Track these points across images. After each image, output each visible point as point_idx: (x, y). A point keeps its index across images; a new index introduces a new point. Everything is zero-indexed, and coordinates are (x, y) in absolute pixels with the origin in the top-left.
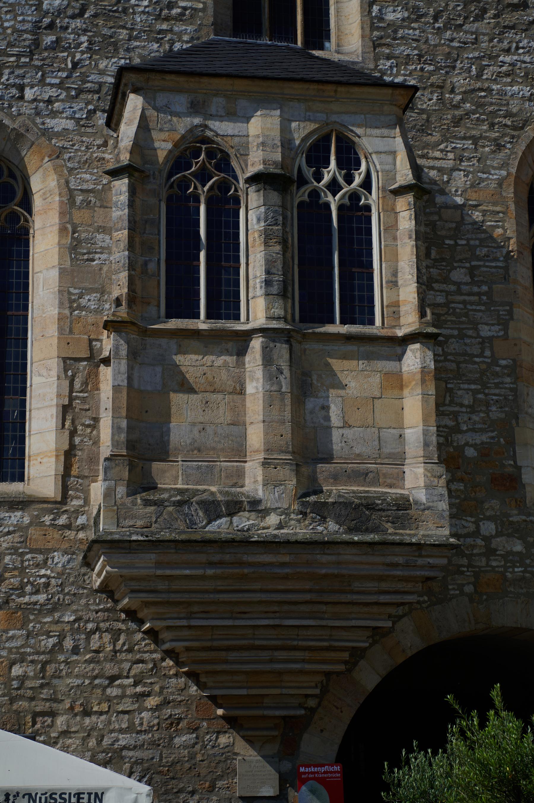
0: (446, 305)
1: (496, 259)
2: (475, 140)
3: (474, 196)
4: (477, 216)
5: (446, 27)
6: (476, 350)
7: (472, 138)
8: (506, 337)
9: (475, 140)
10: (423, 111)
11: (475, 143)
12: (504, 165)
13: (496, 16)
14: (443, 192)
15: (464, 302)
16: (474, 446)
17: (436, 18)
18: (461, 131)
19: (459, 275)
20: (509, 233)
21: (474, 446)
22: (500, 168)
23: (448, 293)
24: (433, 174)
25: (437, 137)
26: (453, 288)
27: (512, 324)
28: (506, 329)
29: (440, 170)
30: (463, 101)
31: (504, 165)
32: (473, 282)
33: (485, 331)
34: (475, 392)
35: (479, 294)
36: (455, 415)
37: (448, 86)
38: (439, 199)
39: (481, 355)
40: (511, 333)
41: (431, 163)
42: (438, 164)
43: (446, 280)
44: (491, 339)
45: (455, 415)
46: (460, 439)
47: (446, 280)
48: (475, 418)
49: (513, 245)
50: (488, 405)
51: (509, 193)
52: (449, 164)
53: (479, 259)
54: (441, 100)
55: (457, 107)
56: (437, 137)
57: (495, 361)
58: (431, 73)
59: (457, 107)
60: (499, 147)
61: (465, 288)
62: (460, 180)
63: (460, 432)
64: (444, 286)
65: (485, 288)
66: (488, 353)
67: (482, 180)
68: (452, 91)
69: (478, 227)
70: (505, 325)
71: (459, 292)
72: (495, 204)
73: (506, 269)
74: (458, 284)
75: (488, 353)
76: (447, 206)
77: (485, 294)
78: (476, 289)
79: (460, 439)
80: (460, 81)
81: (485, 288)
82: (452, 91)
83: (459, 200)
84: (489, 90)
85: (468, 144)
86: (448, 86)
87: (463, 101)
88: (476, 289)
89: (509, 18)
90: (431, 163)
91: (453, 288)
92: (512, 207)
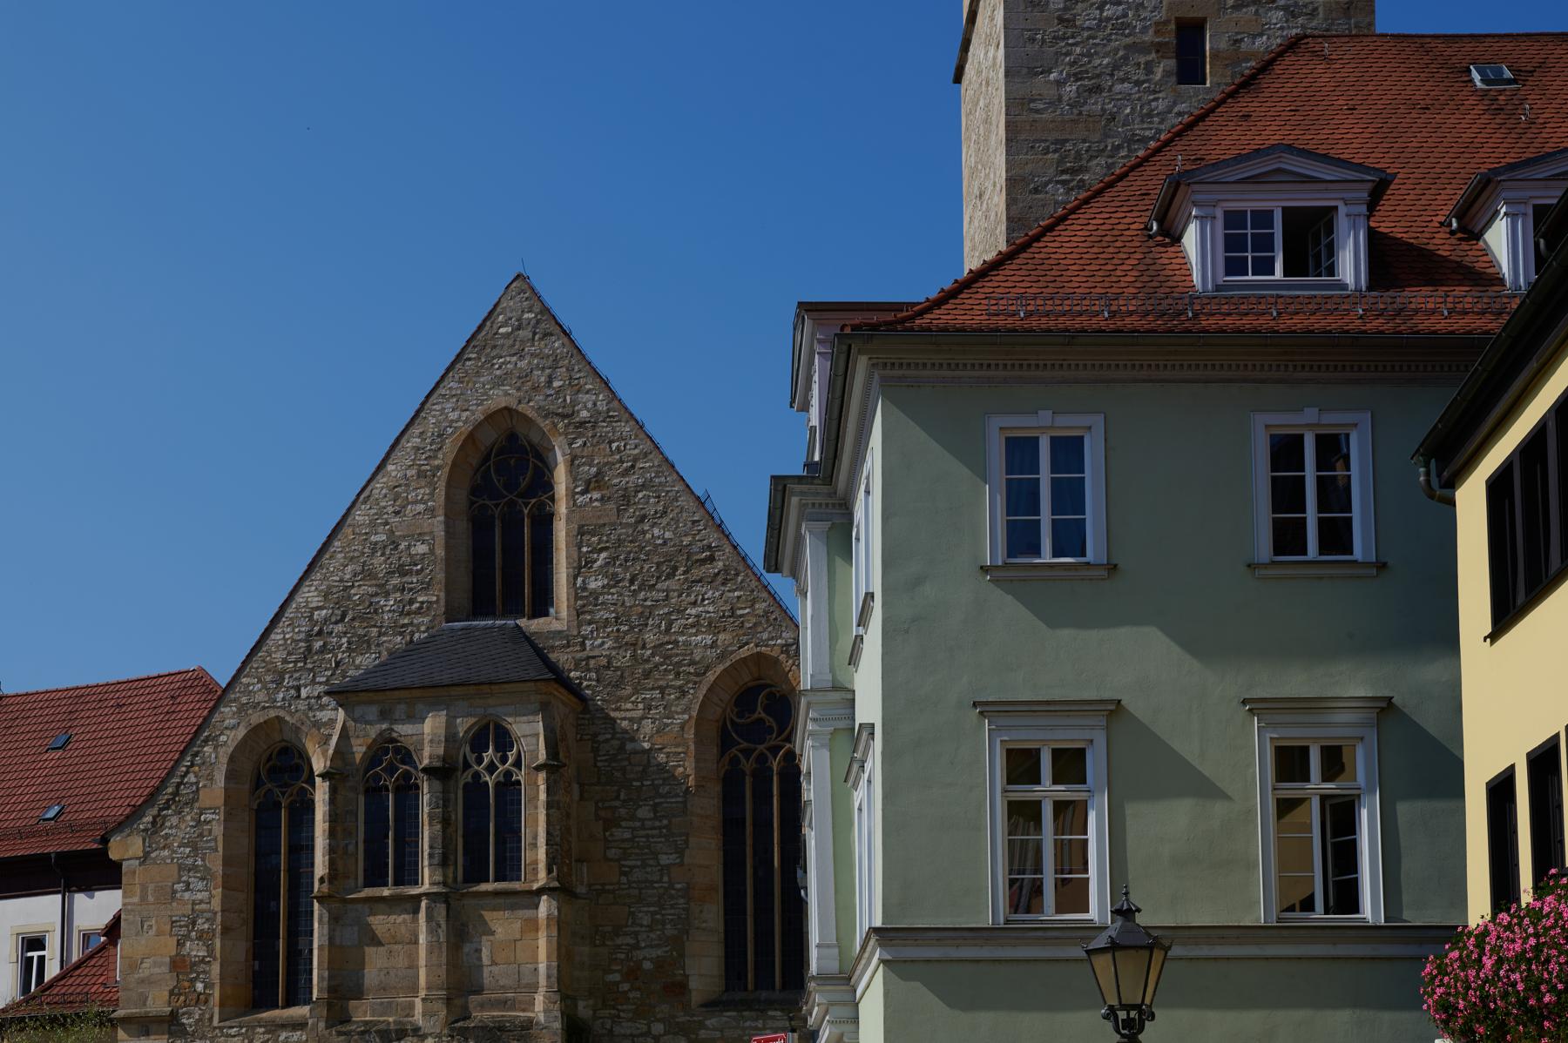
0: (632, 840)
1: (677, 795)
2: (662, 690)
3: (660, 740)
4: (662, 757)
5: (640, 590)
6: (656, 878)
7: (659, 687)
8: (681, 864)
9: (662, 690)
10: (617, 668)
11: (662, 693)
12: (687, 710)
13: (685, 573)
14: (633, 740)
15: (647, 836)
16: (651, 960)
17: (632, 582)
18: (650, 683)
19: (644, 812)
20: (689, 771)
21: (651, 960)
22: (683, 713)
23: (634, 829)
24: (625, 724)
25: (629, 690)
26: (638, 824)
27: (687, 852)
28: (682, 855)
29: (631, 720)
30: (653, 655)
31: (687, 710)
32: (656, 818)
33: (664, 860)
34: (653, 913)
35: (660, 828)
36: (636, 934)
37: (640, 643)
38: (629, 746)
39: (661, 881)
40: (686, 860)
41: (623, 714)
42: (629, 715)
43: (633, 818)
44: (668, 866)
45: (636, 934)
46: (639, 954)
47: (633, 818)
48: (652, 935)
49: (691, 781)
50: (663, 923)
51: (690, 735)
52: (639, 714)
53: (662, 796)
54: (634, 656)
55: (647, 661)
56: (629, 690)
57: (671, 886)
58: (626, 633)
59: (647, 661)
60: (684, 693)
61: (648, 824)
62: (648, 727)
63: (639, 948)
64: (631, 824)
65: (665, 822)
66: (666, 879)
67: (667, 725)
68: (644, 647)
69: (662, 768)
70: (681, 853)
71: (643, 828)
72: (677, 746)
73: (685, 803)
74: (642, 820)
75: (666, 879)
76: (636, 752)
77: (665, 827)
78: (657, 824)
79: (639, 954)
80: (650, 637)
81: (665, 822)
82: (644, 647)
83: (646, 745)
84: (676, 642)
85: (657, 694)
86: (640, 643)
87: (653, 655)
88: (657, 824)
89: (697, 573)
90: (623, 714)
91: (638, 824)
92: (692, 747)
